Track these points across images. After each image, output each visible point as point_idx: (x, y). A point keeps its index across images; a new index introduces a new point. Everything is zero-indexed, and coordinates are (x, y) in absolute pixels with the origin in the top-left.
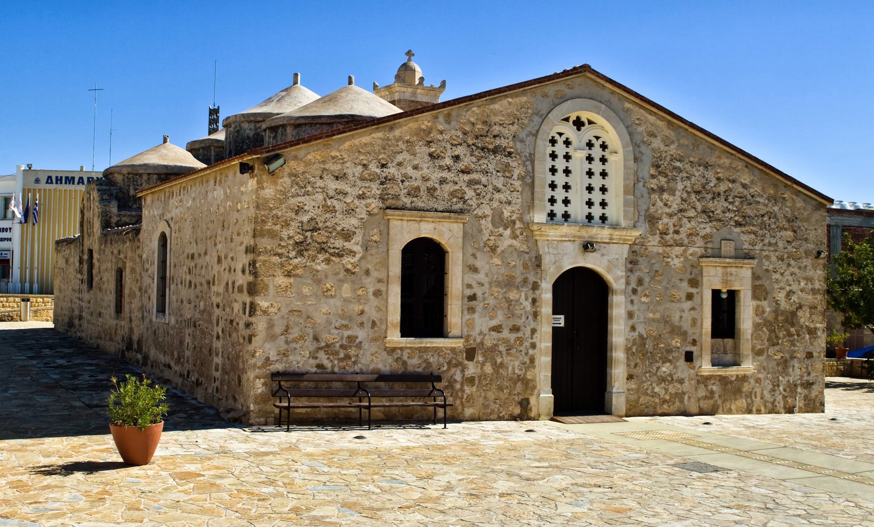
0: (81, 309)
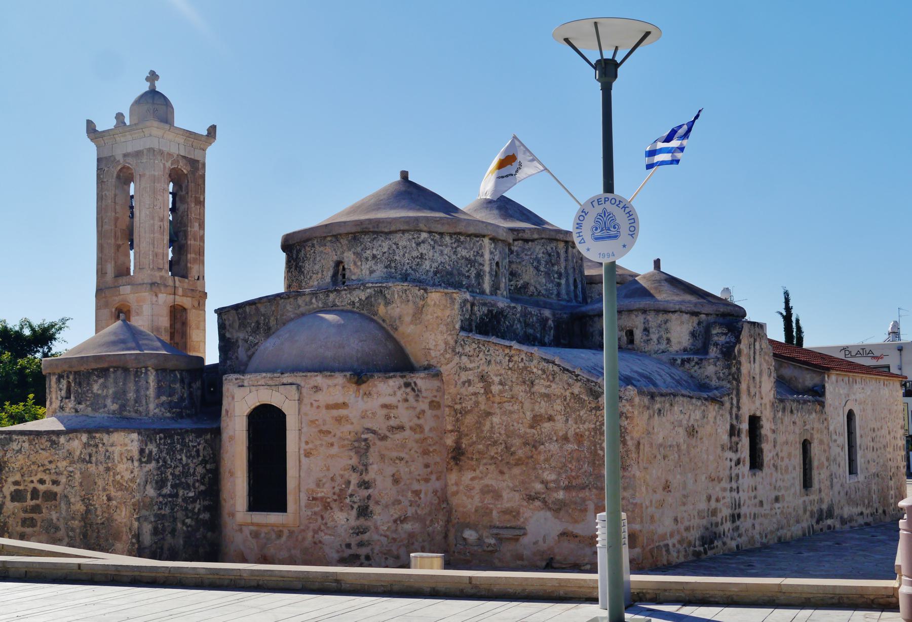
0: (737, 505)
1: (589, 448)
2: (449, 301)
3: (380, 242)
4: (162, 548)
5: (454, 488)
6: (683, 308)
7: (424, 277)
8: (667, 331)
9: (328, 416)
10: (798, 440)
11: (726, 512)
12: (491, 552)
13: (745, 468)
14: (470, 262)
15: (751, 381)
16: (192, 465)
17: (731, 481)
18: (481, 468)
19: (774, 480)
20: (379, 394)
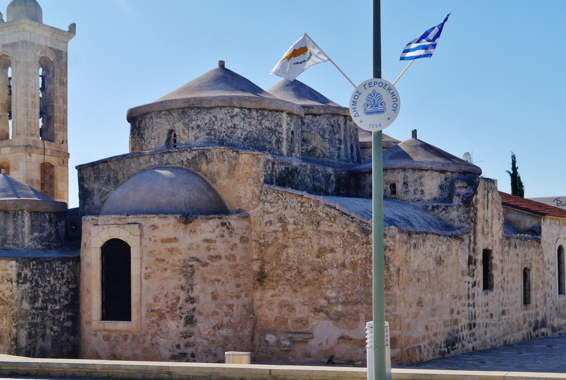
0: (473, 316)
1: (361, 273)
2: (255, 161)
3: (203, 115)
4: (35, 349)
5: (259, 303)
6: (434, 168)
7: (236, 142)
8: (421, 184)
9: (163, 248)
10: (520, 268)
11: (465, 322)
12: (287, 351)
13: (479, 289)
14: (272, 131)
15: (485, 223)
16: (58, 285)
17: (469, 298)
18: (279, 288)
19: (501, 298)
20: (202, 232)
